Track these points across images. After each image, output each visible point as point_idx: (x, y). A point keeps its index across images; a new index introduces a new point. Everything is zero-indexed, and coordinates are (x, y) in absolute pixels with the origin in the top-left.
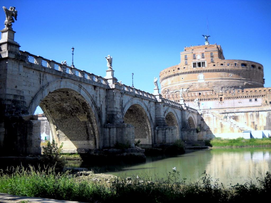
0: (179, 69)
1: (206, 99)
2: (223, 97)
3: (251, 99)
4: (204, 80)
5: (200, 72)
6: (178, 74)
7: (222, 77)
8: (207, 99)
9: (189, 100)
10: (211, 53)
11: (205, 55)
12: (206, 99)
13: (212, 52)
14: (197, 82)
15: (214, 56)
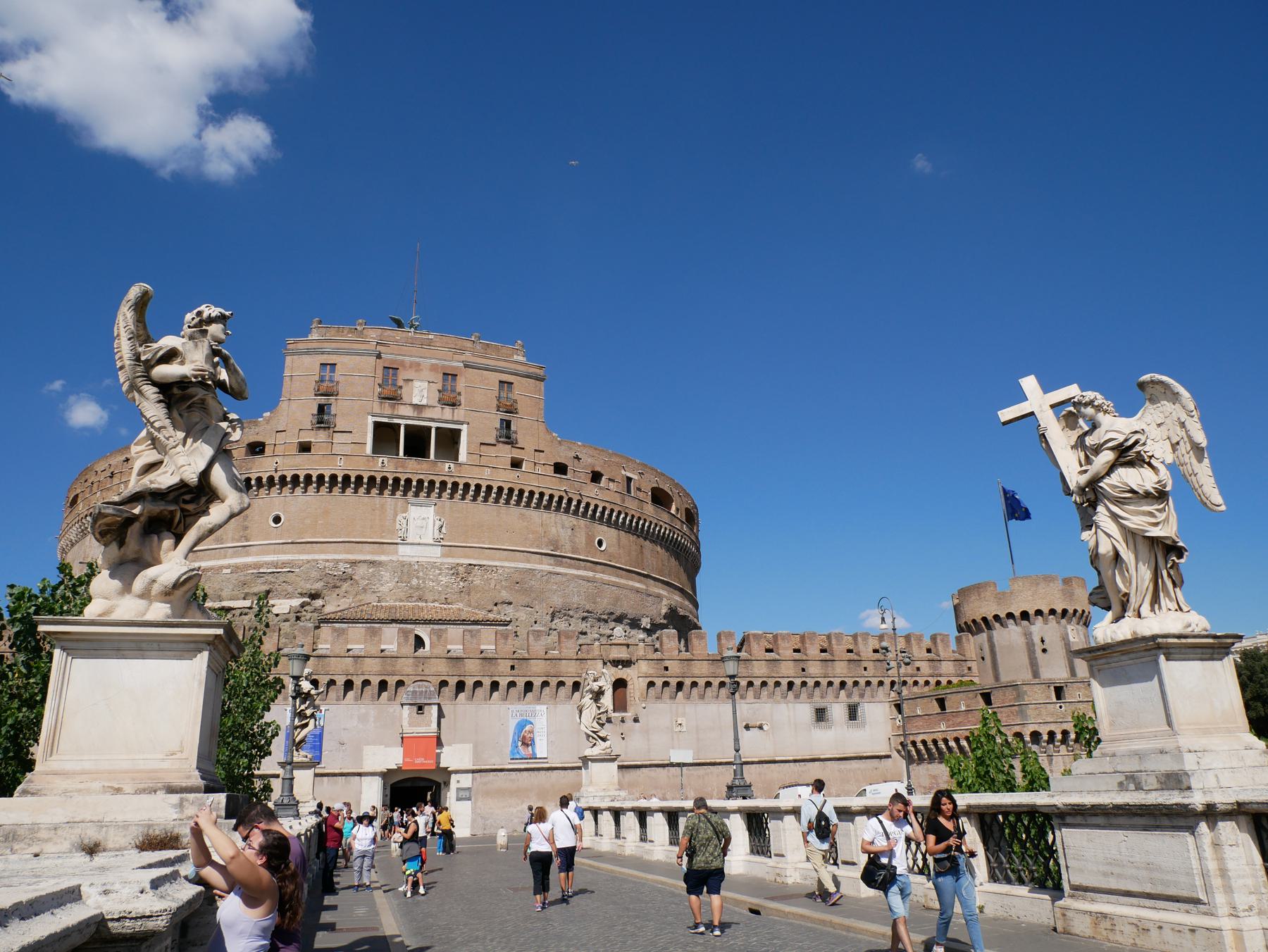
0: (256, 449)
2: (635, 678)
3: (821, 705)
4: (437, 551)
7: (555, 544)
8: (512, 684)
9: (358, 682)
11: (461, 384)
12: (503, 682)
14: (394, 558)
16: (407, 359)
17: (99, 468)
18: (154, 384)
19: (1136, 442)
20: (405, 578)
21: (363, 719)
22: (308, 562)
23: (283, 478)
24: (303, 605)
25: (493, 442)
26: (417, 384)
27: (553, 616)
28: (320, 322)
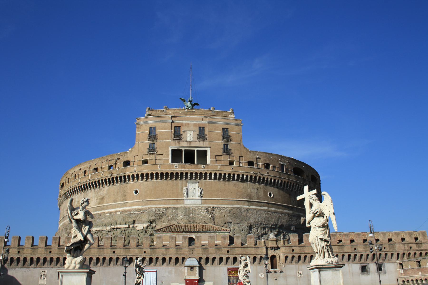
0: (127, 163)
1: (225, 258)
2: (280, 254)
5: (191, 178)
6: (123, 179)
7: (249, 196)
8: (228, 258)
9: (167, 259)
10: (225, 131)
11: (207, 131)
12: (225, 258)
13: (225, 126)
14: (182, 206)
15: (233, 138)
16: (184, 122)
17: (71, 171)
18: (74, 219)
19: (318, 212)
20: (187, 214)
21: (170, 273)
22: (149, 208)
23: (138, 175)
24: (147, 227)
25: (221, 154)
26: (188, 132)
27: (250, 228)
28: (149, 109)
